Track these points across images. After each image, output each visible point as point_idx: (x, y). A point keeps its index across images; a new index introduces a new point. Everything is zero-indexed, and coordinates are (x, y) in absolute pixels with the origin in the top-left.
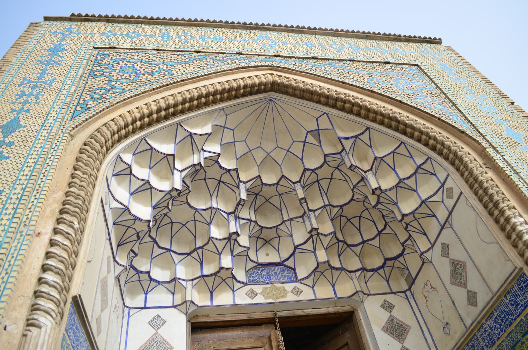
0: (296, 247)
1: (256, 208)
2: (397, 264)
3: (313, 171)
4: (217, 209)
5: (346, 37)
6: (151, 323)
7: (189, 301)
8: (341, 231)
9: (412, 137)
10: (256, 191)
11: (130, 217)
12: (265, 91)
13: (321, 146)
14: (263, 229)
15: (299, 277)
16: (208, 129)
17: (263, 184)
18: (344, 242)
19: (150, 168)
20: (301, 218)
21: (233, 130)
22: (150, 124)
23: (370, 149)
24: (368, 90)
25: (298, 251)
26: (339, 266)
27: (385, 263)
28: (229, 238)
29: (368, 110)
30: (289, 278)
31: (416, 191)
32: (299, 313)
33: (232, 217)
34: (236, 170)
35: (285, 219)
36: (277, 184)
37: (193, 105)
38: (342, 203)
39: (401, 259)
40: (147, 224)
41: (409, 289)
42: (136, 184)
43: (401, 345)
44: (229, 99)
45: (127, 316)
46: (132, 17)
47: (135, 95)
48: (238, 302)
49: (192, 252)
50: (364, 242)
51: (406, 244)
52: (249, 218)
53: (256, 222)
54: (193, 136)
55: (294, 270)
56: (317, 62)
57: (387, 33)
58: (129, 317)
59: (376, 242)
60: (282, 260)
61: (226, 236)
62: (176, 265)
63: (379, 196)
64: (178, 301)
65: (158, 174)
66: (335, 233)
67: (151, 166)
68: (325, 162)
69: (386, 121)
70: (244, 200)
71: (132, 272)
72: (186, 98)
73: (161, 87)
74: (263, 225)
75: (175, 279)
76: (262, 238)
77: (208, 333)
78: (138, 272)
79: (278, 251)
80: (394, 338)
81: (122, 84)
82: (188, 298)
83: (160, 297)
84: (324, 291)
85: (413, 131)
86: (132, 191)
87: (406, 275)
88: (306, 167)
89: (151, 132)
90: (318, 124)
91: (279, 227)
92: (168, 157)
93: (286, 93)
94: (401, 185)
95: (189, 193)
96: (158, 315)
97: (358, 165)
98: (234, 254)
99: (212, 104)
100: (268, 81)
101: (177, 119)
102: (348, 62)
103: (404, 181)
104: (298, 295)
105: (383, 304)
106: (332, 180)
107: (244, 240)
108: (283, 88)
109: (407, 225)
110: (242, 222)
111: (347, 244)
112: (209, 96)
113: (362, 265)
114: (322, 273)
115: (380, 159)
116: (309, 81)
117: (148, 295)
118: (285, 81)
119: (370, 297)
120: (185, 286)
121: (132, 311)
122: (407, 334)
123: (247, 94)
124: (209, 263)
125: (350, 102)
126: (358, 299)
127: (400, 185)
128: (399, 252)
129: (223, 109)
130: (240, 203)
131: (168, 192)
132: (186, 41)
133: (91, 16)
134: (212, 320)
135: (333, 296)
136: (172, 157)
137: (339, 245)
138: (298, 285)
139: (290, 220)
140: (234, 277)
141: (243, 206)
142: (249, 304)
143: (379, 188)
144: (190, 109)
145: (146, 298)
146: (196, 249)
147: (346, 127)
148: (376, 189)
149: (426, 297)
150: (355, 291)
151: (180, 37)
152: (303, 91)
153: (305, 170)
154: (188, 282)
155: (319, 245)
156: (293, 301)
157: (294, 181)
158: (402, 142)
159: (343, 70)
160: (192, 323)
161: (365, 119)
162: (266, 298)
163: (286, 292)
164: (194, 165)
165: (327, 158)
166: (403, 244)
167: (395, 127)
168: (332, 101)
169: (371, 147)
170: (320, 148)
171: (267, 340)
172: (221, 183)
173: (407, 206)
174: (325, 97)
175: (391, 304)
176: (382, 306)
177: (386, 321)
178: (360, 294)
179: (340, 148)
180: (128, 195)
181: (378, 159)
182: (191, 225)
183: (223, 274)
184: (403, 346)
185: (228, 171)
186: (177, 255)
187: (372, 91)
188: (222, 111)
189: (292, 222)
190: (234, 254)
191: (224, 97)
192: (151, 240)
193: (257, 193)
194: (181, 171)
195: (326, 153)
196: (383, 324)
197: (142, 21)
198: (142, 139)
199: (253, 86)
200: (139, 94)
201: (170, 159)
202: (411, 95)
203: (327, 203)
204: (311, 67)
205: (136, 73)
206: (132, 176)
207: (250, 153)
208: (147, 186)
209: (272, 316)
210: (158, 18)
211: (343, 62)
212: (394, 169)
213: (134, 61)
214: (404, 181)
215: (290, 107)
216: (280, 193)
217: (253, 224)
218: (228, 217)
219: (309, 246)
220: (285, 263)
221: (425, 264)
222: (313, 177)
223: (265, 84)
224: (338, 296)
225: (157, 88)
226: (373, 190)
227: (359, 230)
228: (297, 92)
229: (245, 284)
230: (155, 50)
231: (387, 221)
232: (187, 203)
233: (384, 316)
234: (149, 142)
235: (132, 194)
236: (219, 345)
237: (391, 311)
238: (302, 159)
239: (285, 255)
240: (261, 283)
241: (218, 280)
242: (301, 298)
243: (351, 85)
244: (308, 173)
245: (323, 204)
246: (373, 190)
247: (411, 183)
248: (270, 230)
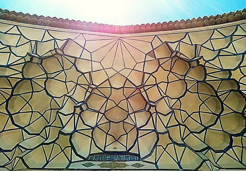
3: (151, 74)
10: (107, 92)
17: (111, 87)
25: (141, 133)
90: (152, 47)
115: (200, 46)
138: (140, 162)
185: (83, 74)
229: (85, 159)
244: (147, 76)
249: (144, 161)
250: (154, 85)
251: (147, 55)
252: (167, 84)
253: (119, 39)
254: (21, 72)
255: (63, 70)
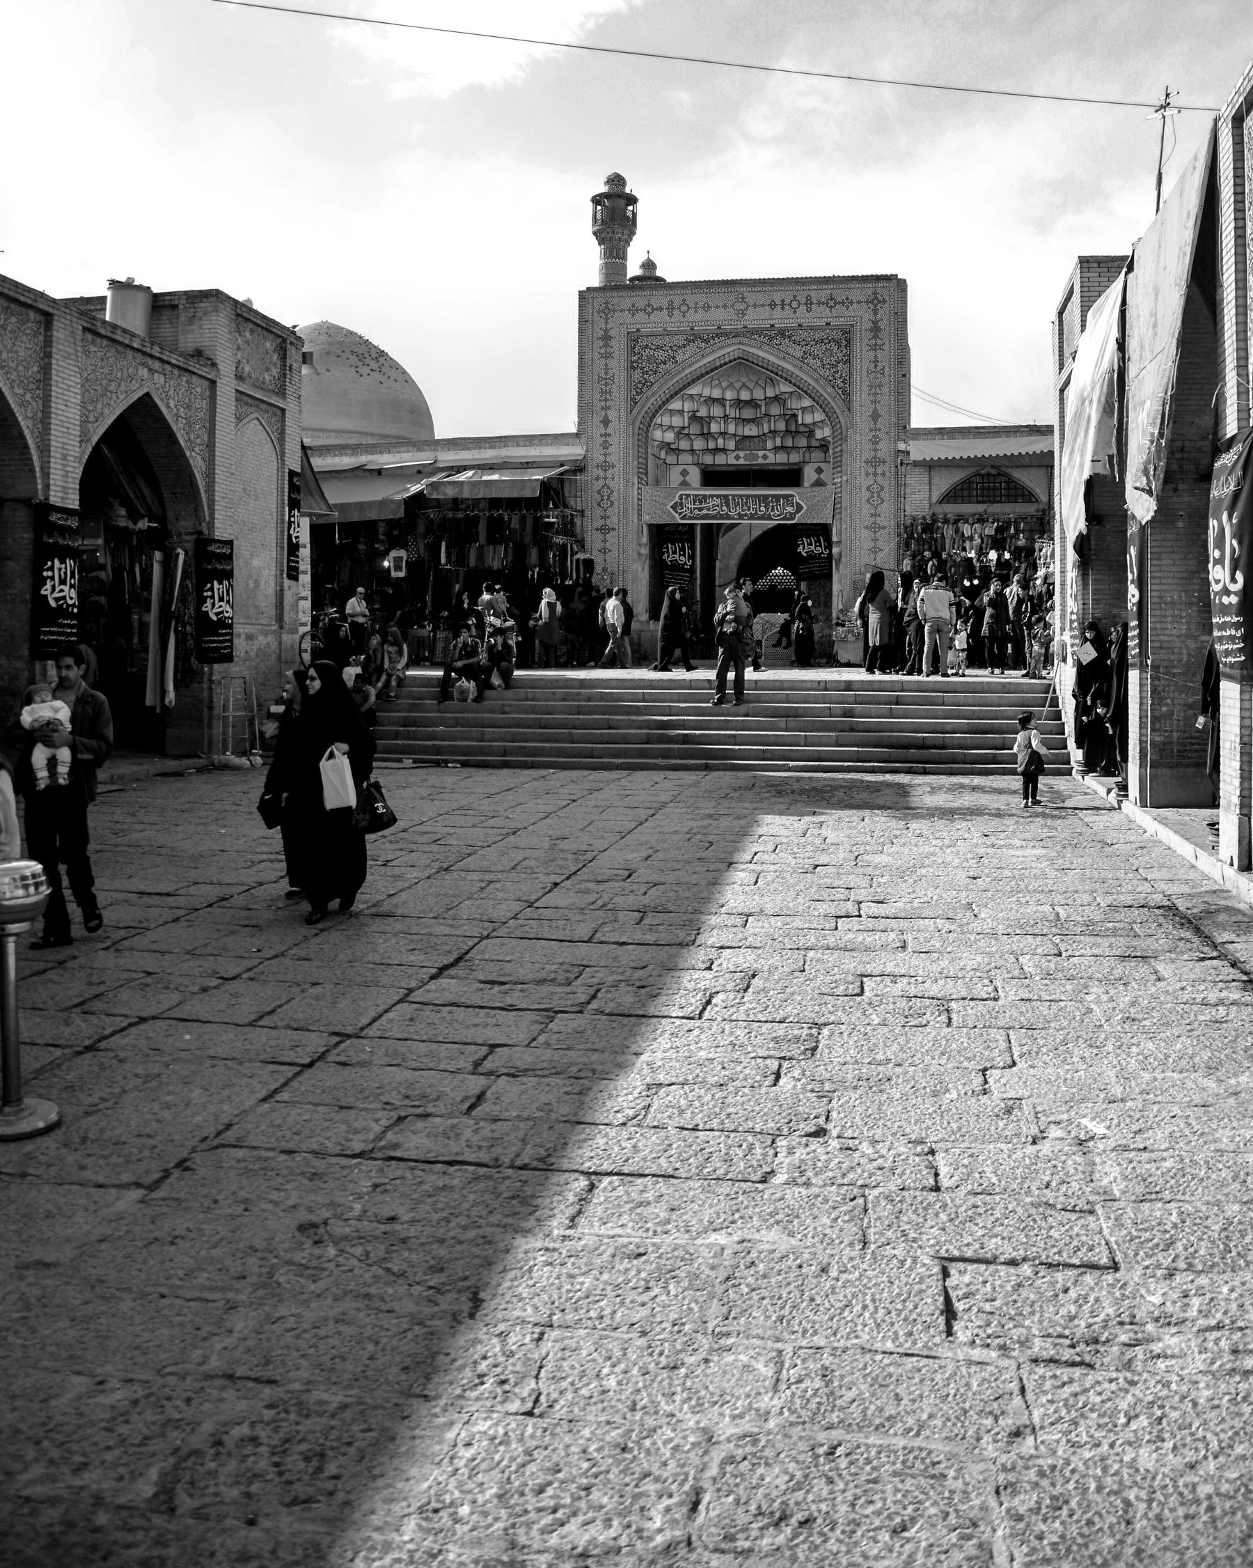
84: (782, 458)
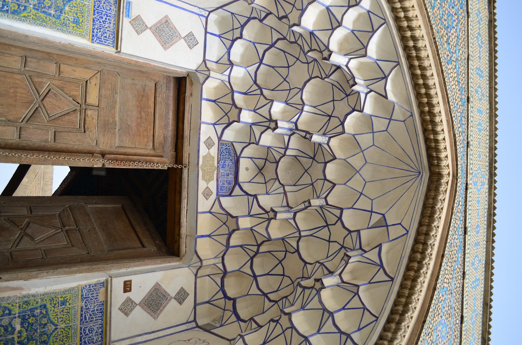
0: (255, 196)
1: (298, 157)
2: (228, 314)
3: (340, 218)
4: (302, 110)
5: (485, 278)
6: (191, 35)
7: (210, 74)
8: (269, 252)
9: (385, 329)
10: (319, 157)
11: (305, 3)
12: (431, 165)
13: (368, 228)
14: (275, 164)
15: (221, 198)
16: (391, 97)
17: (326, 163)
18: (257, 253)
19: (352, 31)
20: (286, 205)
21: (386, 130)
22: (400, 29)
23: (367, 282)
24: (436, 284)
25: (251, 198)
26: (231, 244)
27: (230, 299)
28: (271, 120)
29: (415, 280)
30: (221, 188)
31: (318, 332)
32: (184, 194)
33: (292, 126)
34: (343, 132)
35: (286, 187)
36: (325, 179)
37: (418, 79)
38: (301, 251)
39: (233, 318)
40: (297, 22)
41: (197, 326)
42: (337, 13)
43: (138, 303)
44: (423, 122)
45: (200, 13)
46: (496, 45)
47: (429, 17)
48: (203, 126)
49: (257, 85)
50: (255, 277)
51: (252, 322)
52: (290, 147)
53: (284, 155)
54: (384, 80)
55: (230, 195)
56: (461, 232)
57: (491, 330)
58: (199, 15)
59: (254, 290)
60: (241, 184)
61: (274, 118)
62: (245, 68)
63: (312, 288)
64: (209, 64)
65: (346, 39)
66: (269, 239)
67: (354, 32)
68: (350, 232)
69: (403, 300)
70: (311, 137)
71: (243, 20)
72: (427, 70)
73: (437, 47)
74: (280, 164)
75: (231, 64)
76: (266, 163)
77: (174, 94)
78: (243, 27)
79: (250, 182)
80: (147, 295)
81: (439, 8)
82: (212, 74)
83: (215, 49)
84: (205, 224)
85: (393, 330)
86: (331, 8)
87: (214, 324)
88: (344, 211)
89: (392, 30)
90: (393, 225)
91: (277, 181)
92: (364, 50)
93: (429, 190)
94: (326, 315)
95: (322, 78)
96: (198, 43)
97: (349, 265)
98: (253, 127)
99: (417, 102)
100: (442, 169)
101: (403, 60)
102: (462, 270)
103: (331, 318)
104: (203, 194)
105: (185, 292)
106: (328, 243)
107: (267, 139)
108: (434, 186)
109: (277, 321)
110: (286, 138)
111: (254, 256)
112: (427, 97)
113: (229, 272)
114: (224, 224)
115: (356, 292)
116: (443, 215)
117: (217, 38)
118: (442, 188)
119: (194, 277)
120: (224, 73)
121: (204, 19)
122: (149, 313)
123: (428, 143)
124: (245, 101)
125: (423, 258)
126: (193, 261)
127: (326, 313)
128: (242, 317)
129: (412, 115)
130: (307, 135)
131: (327, 48)
132: (477, 92)
133: (494, 6)
134: (187, 99)
135: (198, 234)
136: (364, 53)
137: (256, 247)
138: (214, 196)
139: (285, 193)
140: (229, 125)
141: (305, 137)
142: (199, 138)
143: (323, 287)
144: (414, 76)
145: (215, 35)
146: (260, 88)
147: (394, 255)
148: (322, 284)
149: (189, 340)
150: (202, 259)
151: (479, 87)
152: (433, 207)
153: (342, 210)
154: (227, 77)
155: (256, 221)
156: (198, 186)
157: (328, 198)
158: (377, 318)
159: (455, 261)
160: (184, 78)
161: (404, 276)
162: (204, 157)
163: (208, 181)
164: (353, 78)
165: (356, 233)
166: (252, 319)
167: (397, 310)
168: (423, 238)
169: (369, 283)
170: (366, 227)
171: (160, 154)
172: (328, 118)
173: (299, 320)
174: (427, 231)
175: (184, 300)
176: (182, 289)
177: (166, 290)
178: (199, 264)
179: (366, 249)
180: (328, 4)
181: (357, 288)
182: (285, 86)
183: (235, 111)
184: (137, 305)
185: (342, 124)
186: (255, 70)
187: (435, 289)
188: (410, 114)
189: (283, 195)
190: (253, 126)
191: (425, 116)
192: (274, 40)
193: (315, 158)
194: (347, 66)
195: (362, 232)
196: (163, 286)
197: (492, 54)
198: (385, 20)
199: (438, 150)
200: (430, 21)
201: (362, 52)
202: (432, 338)
203: (303, 234)
204: (457, 223)
205: (448, 27)
206: (347, 8)
207: (359, 151)
208: (335, 24)
209: (184, 163)
210: (496, 71)
211: (462, 264)
212: (343, 308)
213: (458, 30)
214: (331, 318)
215: (413, 194)
216: (314, 184)
217: (282, 151)
218: (293, 122)
219: (256, 210)
220: (237, 186)
221: (228, 342)
222: (332, 219)
223: (438, 165)
224: (198, 239)
225: (435, 42)
226: (321, 279)
227: (268, 274)
228: (431, 201)
229: (220, 139)
230: (468, 56)
231: (280, 303)
232: (311, 78)
233: (172, 290)
234: (381, 29)
235: (328, 8)
236: (161, 103)
237: (175, 299)
238: (352, 208)
239: (246, 187)
240: (219, 156)
241: (227, 108)
242: (201, 197)
243: (441, 265)
244: (337, 212)
245: (301, 228)
246: (321, 279)
247: (329, 326)
248: (274, 171)
249: (215, 200)
250: (326, 222)
251: (381, 216)
252: (328, 239)
253: (420, 173)
254: (311, 48)
255: (347, 96)
